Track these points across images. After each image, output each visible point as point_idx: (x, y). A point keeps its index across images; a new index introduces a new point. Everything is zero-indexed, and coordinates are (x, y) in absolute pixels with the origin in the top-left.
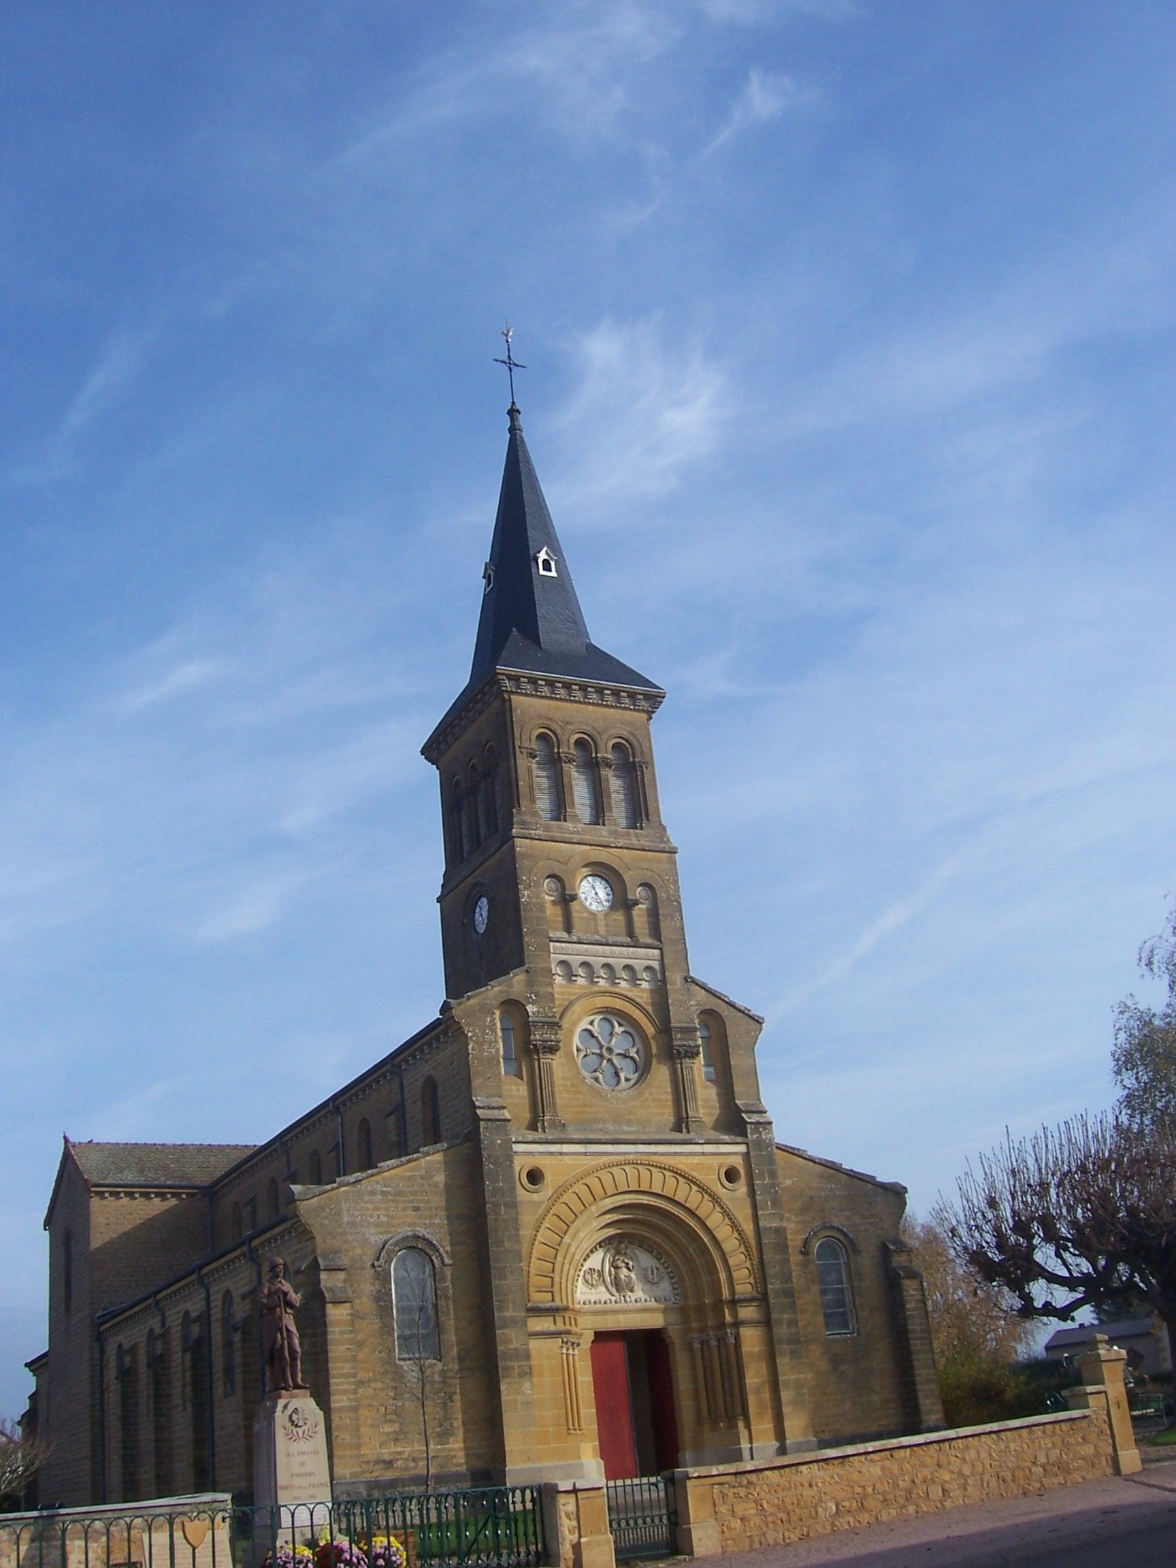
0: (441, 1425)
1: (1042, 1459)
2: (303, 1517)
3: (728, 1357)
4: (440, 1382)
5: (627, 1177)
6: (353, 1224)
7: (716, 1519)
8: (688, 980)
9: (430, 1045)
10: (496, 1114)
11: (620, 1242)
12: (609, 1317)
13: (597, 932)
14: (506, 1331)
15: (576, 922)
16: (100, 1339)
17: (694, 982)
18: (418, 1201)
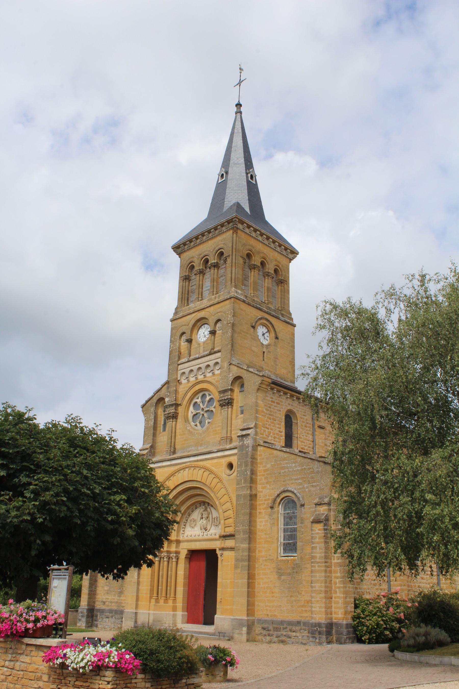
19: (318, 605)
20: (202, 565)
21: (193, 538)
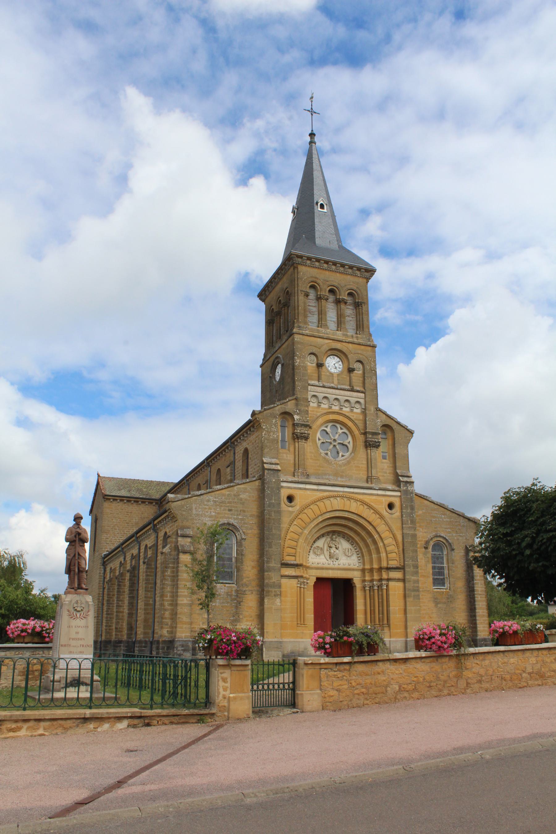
0: (234, 616)
1: (529, 670)
2: (74, 664)
3: (382, 595)
4: (235, 596)
5: (337, 504)
6: (198, 515)
7: (321, 689)
8: (378, 410)
9: (247, 433)
10: (273, 467)
11: (333, 535)
12: (324, 571)
13: (333, 383)
14: (270, 573)
15: (323, 377)
16: (104, 564)
17: (380, 410)
18: (231, 507)
19: (481, 626)
20: (328, 591)
21: (320, 565)
